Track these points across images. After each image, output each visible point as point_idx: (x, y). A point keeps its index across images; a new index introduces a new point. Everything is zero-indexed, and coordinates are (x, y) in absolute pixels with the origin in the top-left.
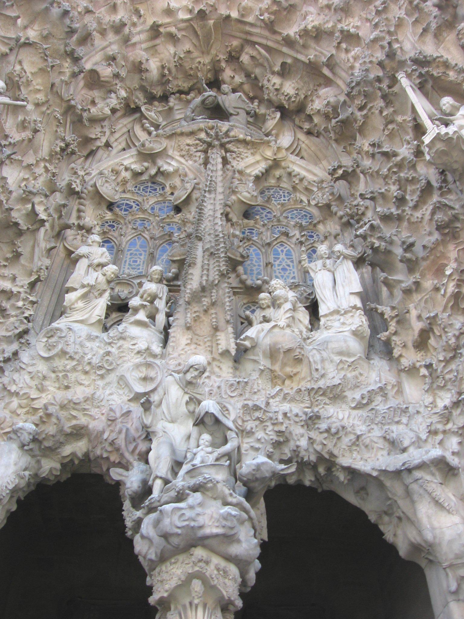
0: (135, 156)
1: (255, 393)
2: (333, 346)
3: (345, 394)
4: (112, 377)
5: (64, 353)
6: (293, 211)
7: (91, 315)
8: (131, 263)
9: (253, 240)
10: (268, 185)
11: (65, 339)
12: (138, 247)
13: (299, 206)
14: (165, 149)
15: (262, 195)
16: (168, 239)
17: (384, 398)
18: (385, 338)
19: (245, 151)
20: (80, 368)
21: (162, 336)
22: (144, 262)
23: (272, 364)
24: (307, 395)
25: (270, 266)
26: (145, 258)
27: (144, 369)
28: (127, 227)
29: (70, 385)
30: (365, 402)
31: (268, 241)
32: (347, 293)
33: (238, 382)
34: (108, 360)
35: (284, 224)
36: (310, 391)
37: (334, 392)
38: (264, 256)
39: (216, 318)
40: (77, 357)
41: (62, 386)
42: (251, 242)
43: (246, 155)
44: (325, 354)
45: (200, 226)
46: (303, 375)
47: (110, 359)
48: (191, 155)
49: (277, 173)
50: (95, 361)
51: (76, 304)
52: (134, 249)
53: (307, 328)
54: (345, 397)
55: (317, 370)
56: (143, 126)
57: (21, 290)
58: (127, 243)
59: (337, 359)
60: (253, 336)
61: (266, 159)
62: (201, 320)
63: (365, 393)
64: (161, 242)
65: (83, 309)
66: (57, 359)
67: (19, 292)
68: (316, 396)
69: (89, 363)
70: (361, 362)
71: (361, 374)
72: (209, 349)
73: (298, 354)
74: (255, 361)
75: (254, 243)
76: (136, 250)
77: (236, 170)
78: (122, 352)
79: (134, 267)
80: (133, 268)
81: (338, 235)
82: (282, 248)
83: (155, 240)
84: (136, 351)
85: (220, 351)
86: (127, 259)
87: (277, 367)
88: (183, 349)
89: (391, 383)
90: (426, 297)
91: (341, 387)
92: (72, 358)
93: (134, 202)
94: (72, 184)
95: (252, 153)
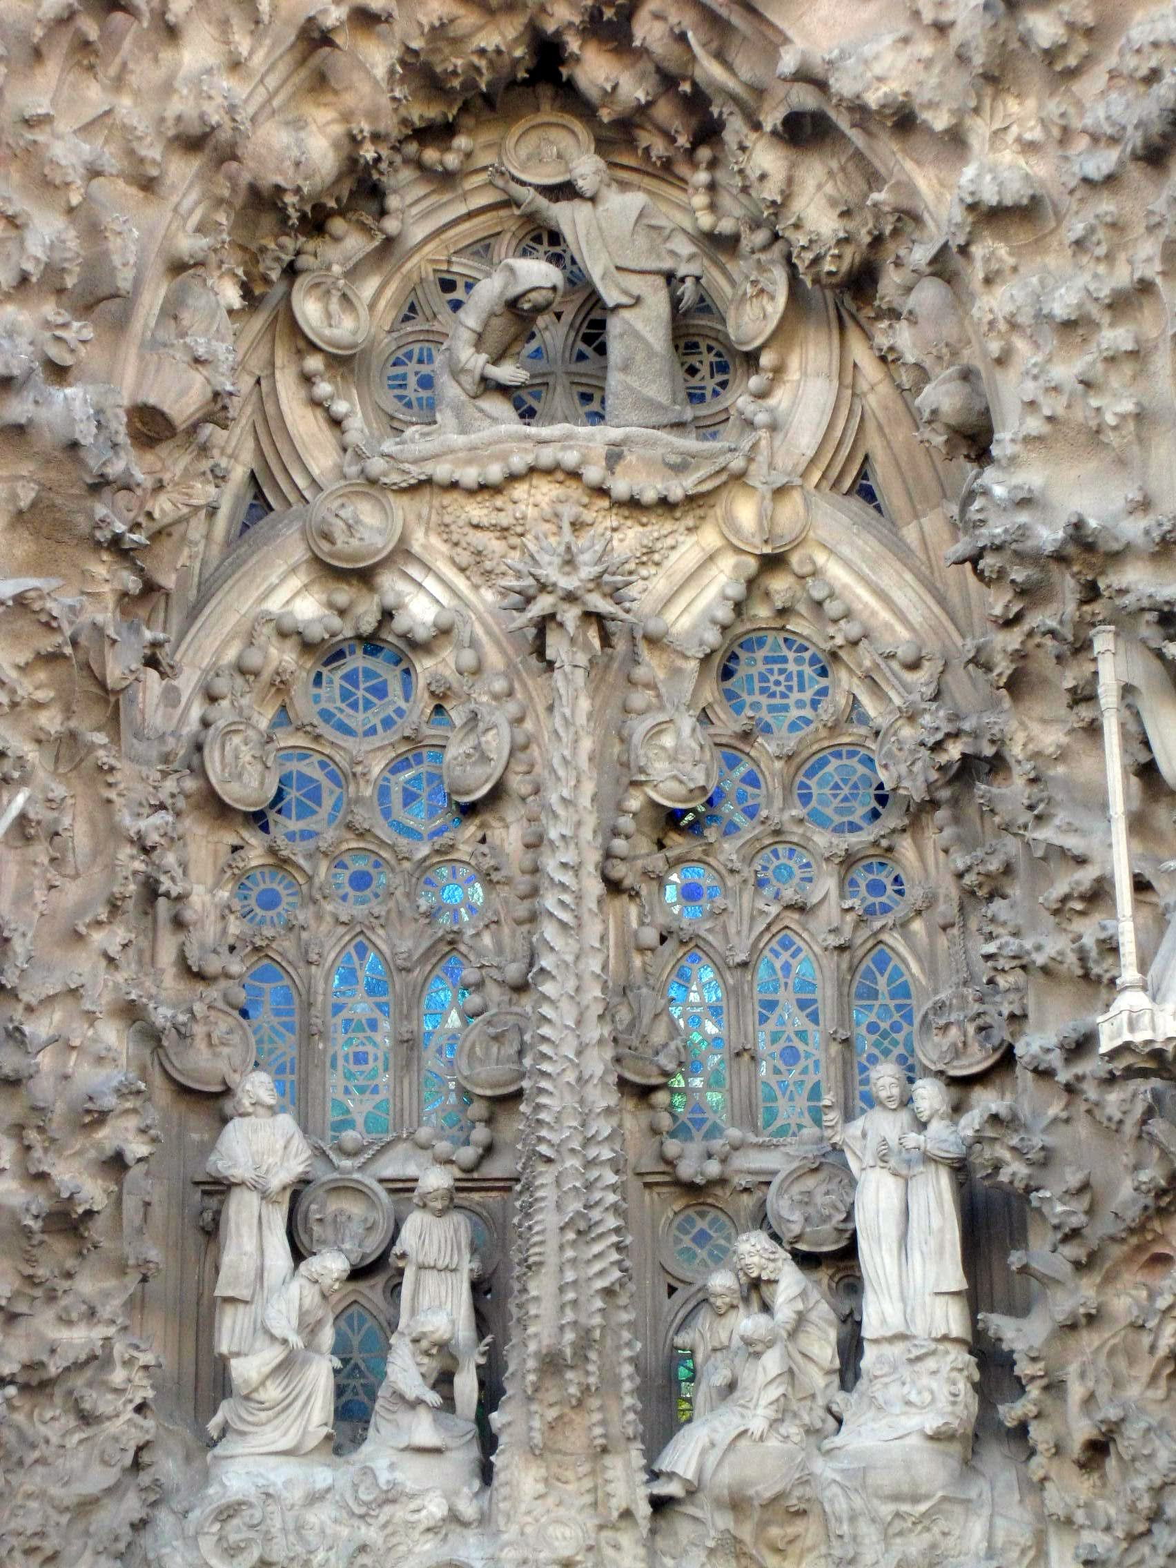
0: (304, 568)
6: (823, 763)
9: (698, 936)
10: (749, 626)
11: (263, 1528)
14: (403, 539)
15: (728, 684)
19: (668, 526)
21: (475, 1452)
25: (746, 1057)
28: (319, 917)
31: (742, 957)
32: (930, 1288)
35: (795, 839)
38: (732, 1002)
39: (603, 1423)
42: (692, 945)
43: (670, 541)
44: (858, 1502)
45: (545, 1106)
46: (809, 1542)
48: (490, 572)
49: (780, 584)
53: (829, 1373)
55: (841, 1537)
56: (307, 379)
57: (111, 1331)
59: (886, 1510)
60: (690, 1475)
61: (738, 551)
64: (429, 967)
65: (283, 1407)
67: (107, 1339)
70: (946, 1506)
71: (945, 1534)
72: (588, 1499)
73: (794, 1501)
74: (695, 1519)
75: (701, 944)
77: (639, 635)
78: (393, 1534)
79: (362, 1082)
81: (953, 925)
83: (408, 970)
84: (422, 1527)
85: (615, 1514)
87: (746, 1532)
88: (529, 1513)
89: (1017, 1544)
90: (1112, 1342)
93: (323, 765)
94: (157, 882)
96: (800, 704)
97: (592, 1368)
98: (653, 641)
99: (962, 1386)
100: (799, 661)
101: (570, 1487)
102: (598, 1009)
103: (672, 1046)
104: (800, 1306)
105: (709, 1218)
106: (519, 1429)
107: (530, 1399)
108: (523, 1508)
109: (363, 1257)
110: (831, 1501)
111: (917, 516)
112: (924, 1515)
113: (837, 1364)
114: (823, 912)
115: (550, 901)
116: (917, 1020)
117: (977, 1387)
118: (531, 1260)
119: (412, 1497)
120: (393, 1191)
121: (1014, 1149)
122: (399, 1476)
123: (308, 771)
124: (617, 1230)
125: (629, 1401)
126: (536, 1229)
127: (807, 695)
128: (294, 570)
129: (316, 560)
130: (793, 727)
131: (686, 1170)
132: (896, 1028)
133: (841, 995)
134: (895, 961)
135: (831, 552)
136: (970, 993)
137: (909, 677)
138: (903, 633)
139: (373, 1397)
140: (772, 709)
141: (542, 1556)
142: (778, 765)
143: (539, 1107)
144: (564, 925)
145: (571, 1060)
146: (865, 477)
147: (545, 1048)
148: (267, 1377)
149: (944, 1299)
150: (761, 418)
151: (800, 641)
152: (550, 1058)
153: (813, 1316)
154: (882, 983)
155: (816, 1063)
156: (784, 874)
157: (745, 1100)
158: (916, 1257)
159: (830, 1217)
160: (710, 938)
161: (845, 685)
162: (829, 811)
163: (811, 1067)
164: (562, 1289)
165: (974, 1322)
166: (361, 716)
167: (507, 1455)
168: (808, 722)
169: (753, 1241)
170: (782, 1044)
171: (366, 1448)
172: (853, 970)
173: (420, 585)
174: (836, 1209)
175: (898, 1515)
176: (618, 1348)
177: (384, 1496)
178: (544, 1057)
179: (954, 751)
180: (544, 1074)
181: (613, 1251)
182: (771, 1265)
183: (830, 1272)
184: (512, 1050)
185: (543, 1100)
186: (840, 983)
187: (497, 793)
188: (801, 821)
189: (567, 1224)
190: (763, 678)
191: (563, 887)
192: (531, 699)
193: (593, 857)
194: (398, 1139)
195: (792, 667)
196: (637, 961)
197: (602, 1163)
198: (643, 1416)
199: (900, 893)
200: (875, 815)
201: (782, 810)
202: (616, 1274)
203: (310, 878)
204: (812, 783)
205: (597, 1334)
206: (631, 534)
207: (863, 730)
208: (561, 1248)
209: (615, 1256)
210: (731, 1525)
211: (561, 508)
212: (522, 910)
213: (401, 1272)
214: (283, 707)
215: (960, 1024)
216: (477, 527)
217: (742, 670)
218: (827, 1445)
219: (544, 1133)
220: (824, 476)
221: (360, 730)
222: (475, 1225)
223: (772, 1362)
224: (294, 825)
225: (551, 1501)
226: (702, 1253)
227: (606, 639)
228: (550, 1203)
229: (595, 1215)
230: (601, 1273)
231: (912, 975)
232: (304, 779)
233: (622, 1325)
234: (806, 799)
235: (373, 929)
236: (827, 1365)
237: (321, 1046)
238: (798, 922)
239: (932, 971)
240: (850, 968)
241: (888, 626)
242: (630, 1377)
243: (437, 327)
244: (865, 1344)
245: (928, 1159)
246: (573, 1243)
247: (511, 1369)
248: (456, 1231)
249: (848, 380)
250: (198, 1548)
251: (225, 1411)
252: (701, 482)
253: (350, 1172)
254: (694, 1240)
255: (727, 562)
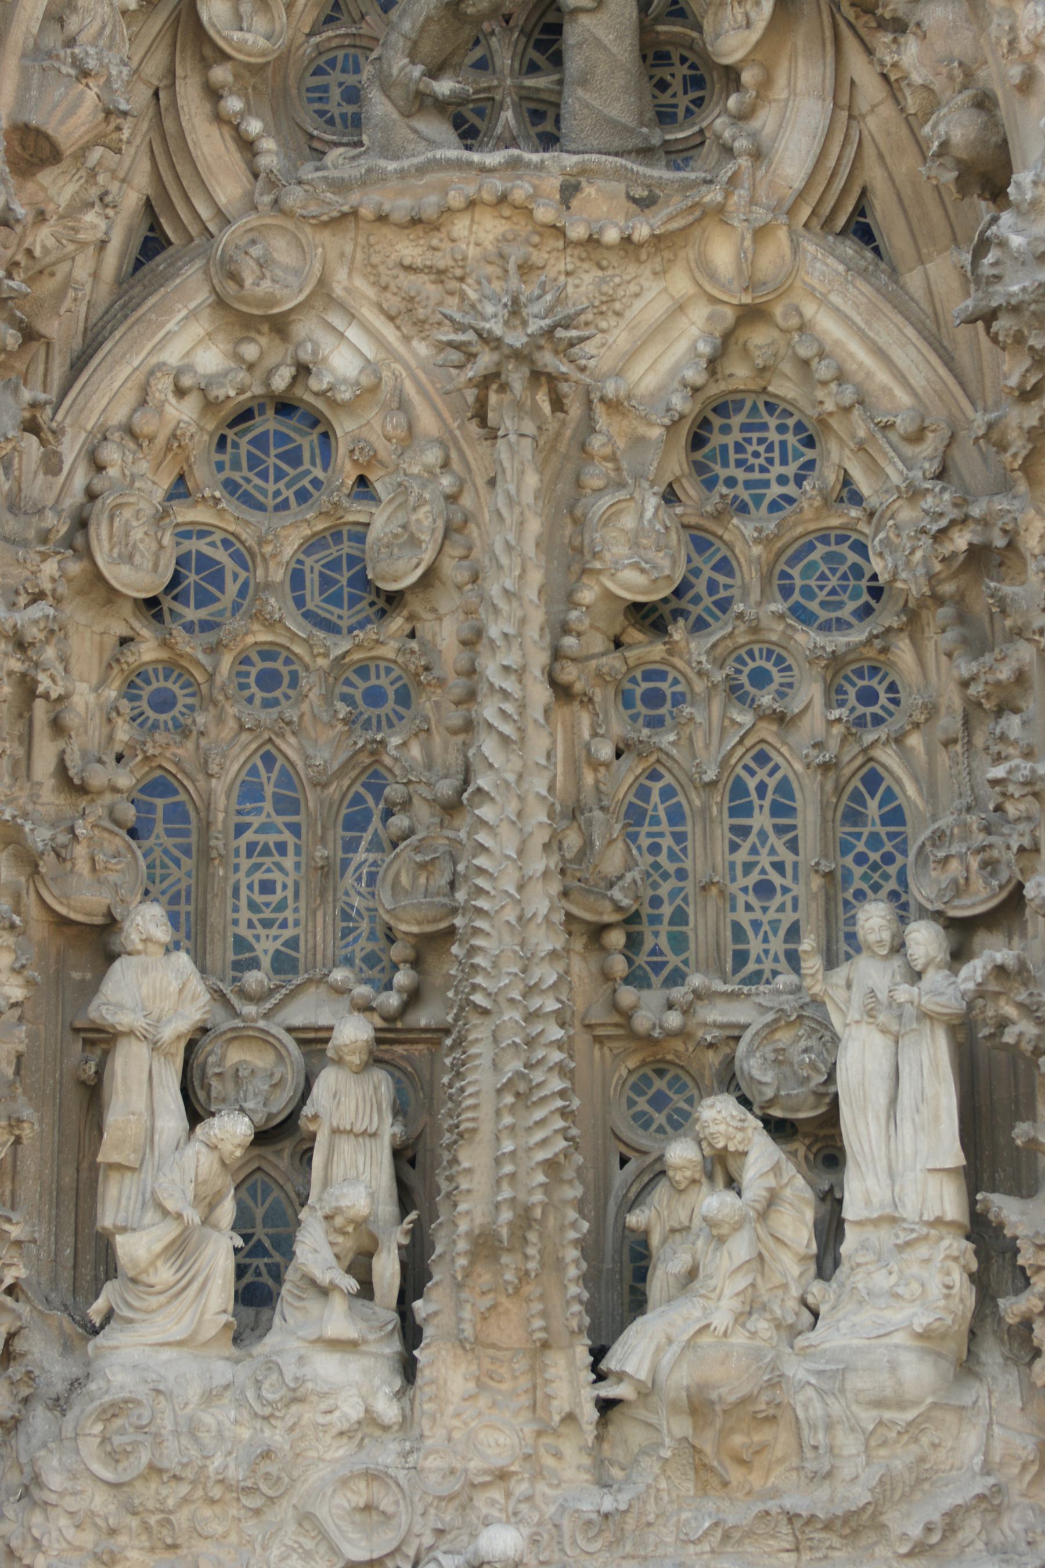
0: (207, 312)
1: (649, 1524)
2: (860, 1385)
3: (884, 1519)
4: (284, 1511)
5: (154, 1470)
6: (810, 547)
7: (202, 1315)
8: (259, 899)
9: (660, 749)
10: (723, 386)
11: (153, 1429)
12: (268, 806)
13: (835, 522)
15: (699, 455)
16: (368, 761)
17: (990, 1517)
18: (1017, 1320)
19: (632, 270)
20: (200, 1493)
21: (395, 1346)
22: (296, 884)
23: (694, 1428)
24: (785, 1521)
25: (714, 890)
26: (297, 866)
27: (362, 1485)
28: (220, 720)
29: (179, 1541)
30: (935, 1538)
33: (606, 1516)
34: (268, 1474)
36: (791, 1518)
37: (853, 1524)
39: (544, 1314)
40: (189, 1474)
41: (160, 1544)
42: (653, 759)
43: (633, 288)
44: (836, 1408)
45: (480, 949)
46: (779, 1453)
47: (273, 1468)
48: (424, 322)
49: (759, 337)
50: (235, 1473)
51: (151, 1270)
52: (256, 821)
53: (804, 1259)
54: (884, 1526)
55: (815, 1448)
58: (228, 795)
59: (868, 1418)
60: (643, 1375)
61: (714, 300)
62: (501, 1309)
63: (936, 1517)
64: (346, 782)
66: (139, 1486)
68: (807, 1530)
69: (221, 1481)
70: (938, 1414)
71: (935, 1446)
73: (763, 1407)
74: (649, 1425)
75: (664, 759)
76: (263, 829)
77: (595, 397)
78: (302, 1437)
79: (267, 914)
80: (267, 924)
81: (955, 741)
82: (762, 774)
83: (325, 786)
84: (335, 1431)
85: (557, 1418)
86: (241, 874)
88: (457, 1415)
91: (871, 1509)
92: (176, 1478)
93: (226, 544)
94: (36, 682)
95: (655, 273)
96: (782, 480)
97: (531, 1251)
98: (613, 405)
99: (958, 1277)
100: (782, 429)
101: (504, 1387)
102: (543, 836)
103: (629, 877)
104: (772, 1182)
105: (668, 1077)
106: (445, 1320)
107: (459, 1286)
108: (450, 1410)
109: (270, 1117)
110: (806, 1407)
111: (921, 261)
112: (910, 1424)
113: (814, 1249)
114: (806, 722)
115: (489, 711)
116: (912, 852)
117: (973, 1277)
118: (462, 1127)
119: (325, 1395)
120: (301, 1042)
121: (1020, 1005)
122: (307, 1371)
123: (208, 551)
124: (562, 1094)
125: (574, 1290)
126: (470, 1090)
127: (791, 470)
128: (193, 314)
129: (220, 303)
130: (774, 506)
131: (642, 1022)
132: (888, 859)
133: (824, 821)
134: (888, 781)
135: (823, 301)
136: (973, 820)
137: (908, 450)
138: (903, 398)
139: (278, 1279)
140: (748, 484)
141: (472, 1465)
142: (757, 550)
143: (473, 951)
144: (505, 739)
145: (511, 896)
146: (863, 213)
147: (482, 882)
148: (158, 1256)
149: (938, 1176)
150: (741, 144)
151: (783, 405)
152: (488, 893)
153: (788, 1192)
154: (873, 807)
155: (795, 900)
156: (760, 678)
157: (711, 940)
158: (906, 1128)
159: (808, 1079)
160: (674, 752)
161: (835, 457)
162: (813, 606)
163: (789, 906)
164: (498, 1161)
165: (973, 1203)
166: (271, 487)
167: (433, 1349)
168: (790, 500)
169: (719, 1106)
170: (755, 877)
171: (271, 1340)
172: (839, 791)
173: (342, 335)
174: (817, 1070)
175: (881, 1423)
176: (562, 1229)
177: (291, 1395)
178: (480, 891)
179: (961, 541)
180: (479, 911)
181: (557, 1116)
182: (739, 1136)
183: (807, 1142)
184: (444, 880)
185: (478, 942)
186: (824, 807)
187: (429, 578)
188: (781, 617)
189: (505, 1085)
190: (739, 448)
191: (505, 694)
192: (469, 470)
193: (540, 659)
194: (310, 981)
195: (773, 436)
196: (589, 779)
197: (548, 1014)
198: (590, 1307)
199: (896, 702)
200: (865, 612)
201: (759, 604)
202: (561, 1144)
203: (211, 677)
204: (795, 572)
205: (538, 1213)
206: (588, 278)
207: (854, 513)
208: (498, 1113)
209: (560, 1124)
210: (690, 1432)
211: (507, 249)
212: (455, 718)
213: (313, 1137)
214: (181, 478)
215: (962, 857)
216: (409, 268)
217: (716, 439)
218: (800, 1342)
219: (479, 980)
220: (814, 213)
221: (270, 503)
222: (397, 1082)
223: (740, 1248)
224: (191, 613)
225: (483, 1402)
226: (660, 1118)
227: (558, 404)
228: (485, 1062)
229: (537, 1076)
230: (544, 1143)
231: (908, 798)
232: (204, 562)
233: (565, 1202)
234: (786, 592)
235: (282, 736)
236: (802, 1251)
237: (221, 873)
238: (777, 735)
239: (931, 795)
240: (836, 788)
241: (886, 390)
242: (576, 1262)
243: (365, 30)
244: (846, 1226)
245: (924, 1016)
246: (512, 1108)
247: (439, 1249)
248: (376, 1089)
249: (844, 100)
250: (77, 1451)
251: (109, 1295)
252: (671, 218)
253: (255, 1020)
254: (650, 1102)
255: (699, 314)
